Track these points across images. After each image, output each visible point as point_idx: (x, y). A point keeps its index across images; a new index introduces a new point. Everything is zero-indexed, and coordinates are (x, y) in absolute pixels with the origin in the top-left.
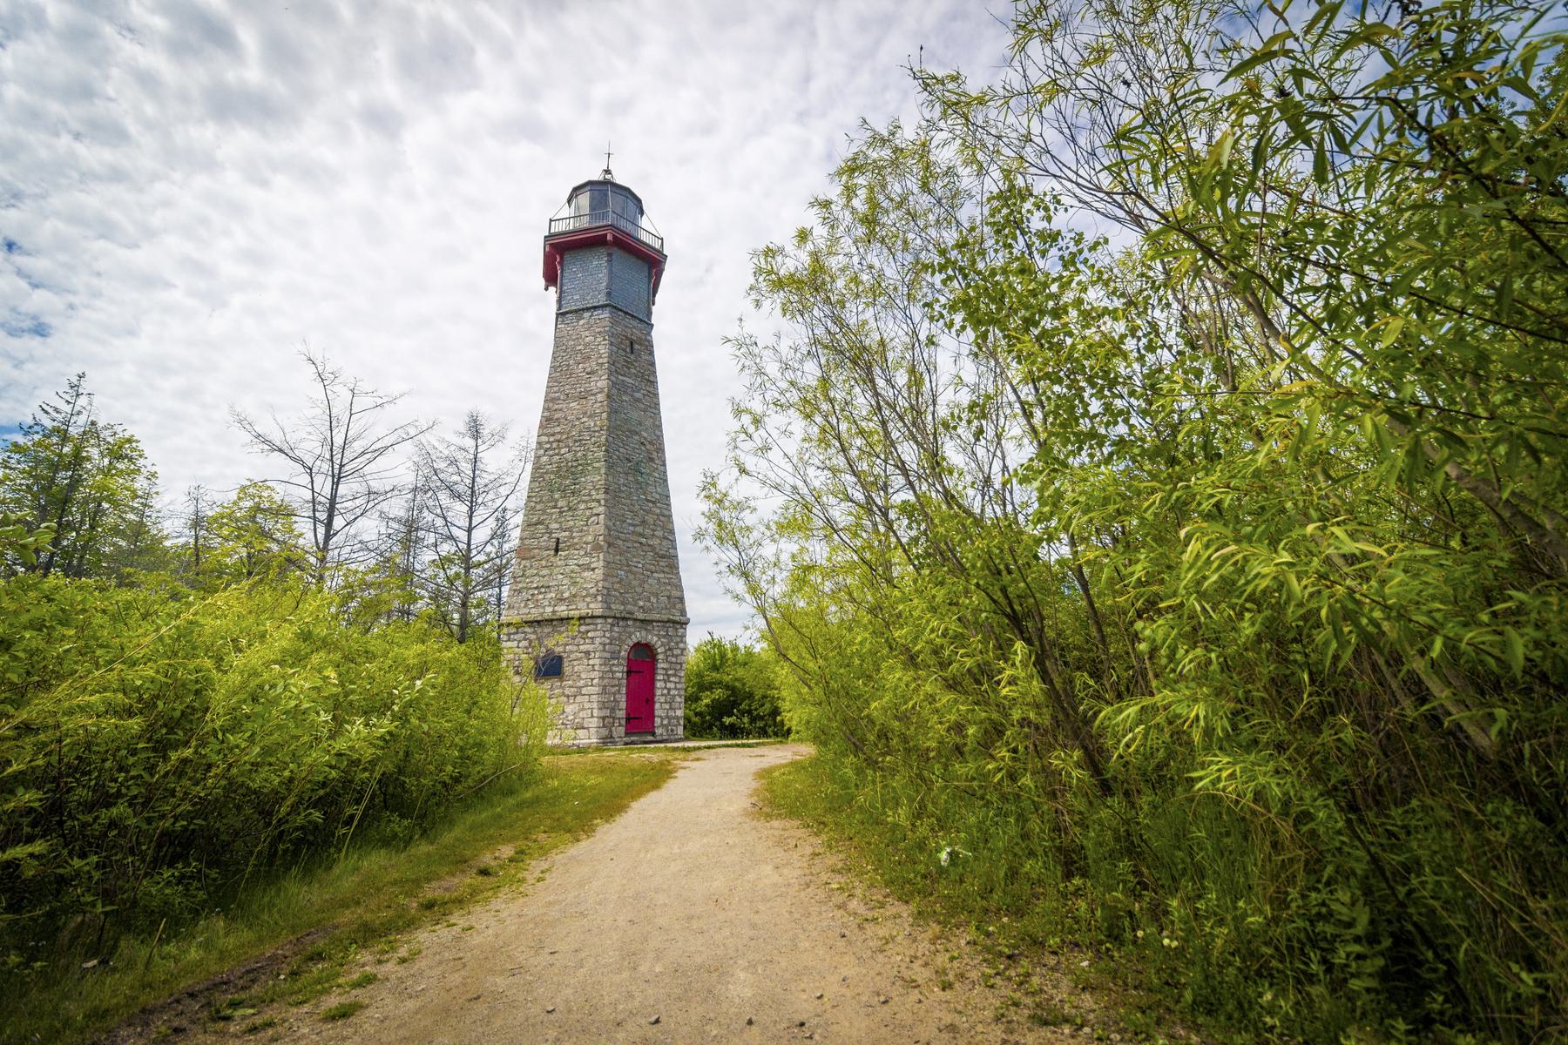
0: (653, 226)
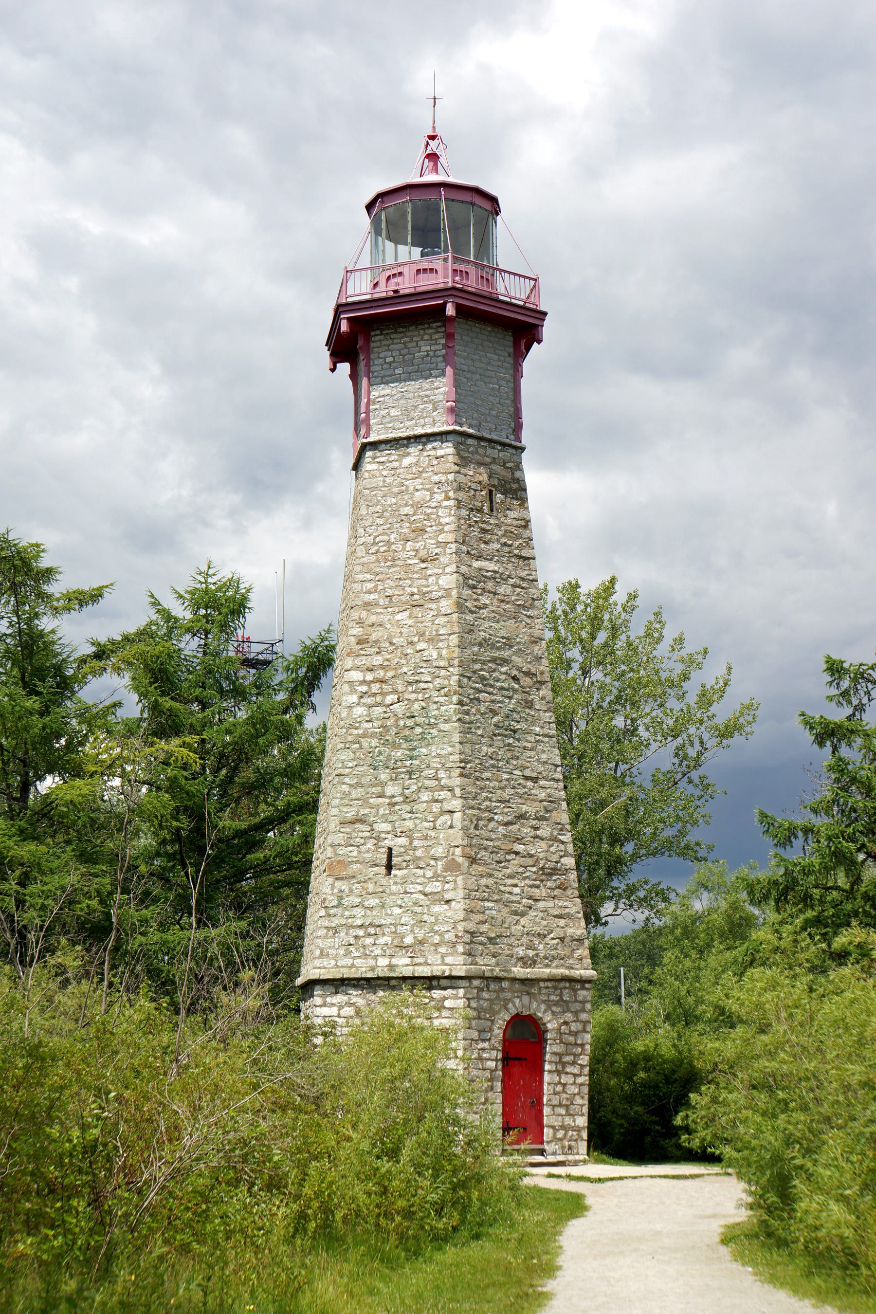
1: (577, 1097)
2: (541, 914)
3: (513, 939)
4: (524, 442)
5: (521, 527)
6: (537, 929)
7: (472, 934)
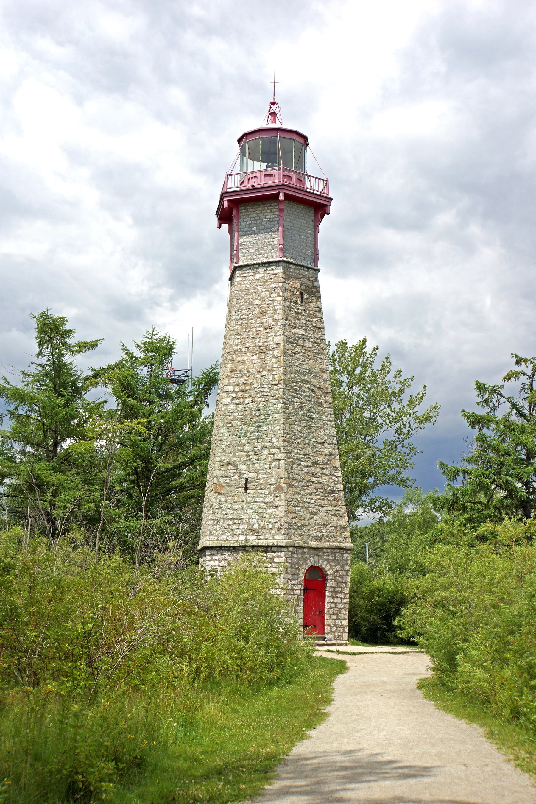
0: (318, 167)
1: (343, 610)
2: (325, 514)
3: (310, 526)
4: (320, 266)
5: (317, 311)
6: (323, 522)
7: (289, 524)
